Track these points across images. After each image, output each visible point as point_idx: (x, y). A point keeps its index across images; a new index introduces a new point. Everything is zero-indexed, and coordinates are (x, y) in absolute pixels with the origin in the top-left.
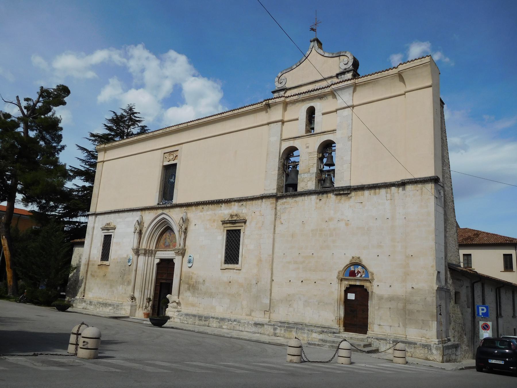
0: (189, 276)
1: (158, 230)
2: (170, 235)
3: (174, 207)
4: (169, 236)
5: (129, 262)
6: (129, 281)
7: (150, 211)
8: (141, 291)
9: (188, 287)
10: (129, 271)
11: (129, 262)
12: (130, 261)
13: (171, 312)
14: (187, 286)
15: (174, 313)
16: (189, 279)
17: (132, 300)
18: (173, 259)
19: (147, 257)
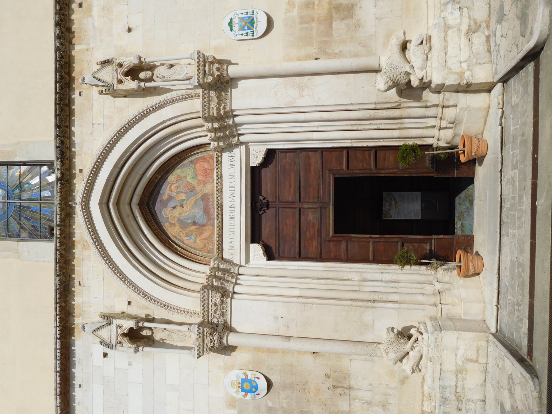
0: (303, 20)
1: (147, 248)
2: (172, 204)
3: (69, 149)
4: (175, 207)
5: (254, 389)
6: (330, 383)
7: (76, 282)
8: (370, 304)
9: (342, 19)
10: (291, 386)
11: (256, 388)
12: (250, 381)
13: (449, 49)
14: (339, 26)
15: (450, 32)
16: (313, 20)
17: (410, 337)
18: (253, 168)
19: (237, 289)
